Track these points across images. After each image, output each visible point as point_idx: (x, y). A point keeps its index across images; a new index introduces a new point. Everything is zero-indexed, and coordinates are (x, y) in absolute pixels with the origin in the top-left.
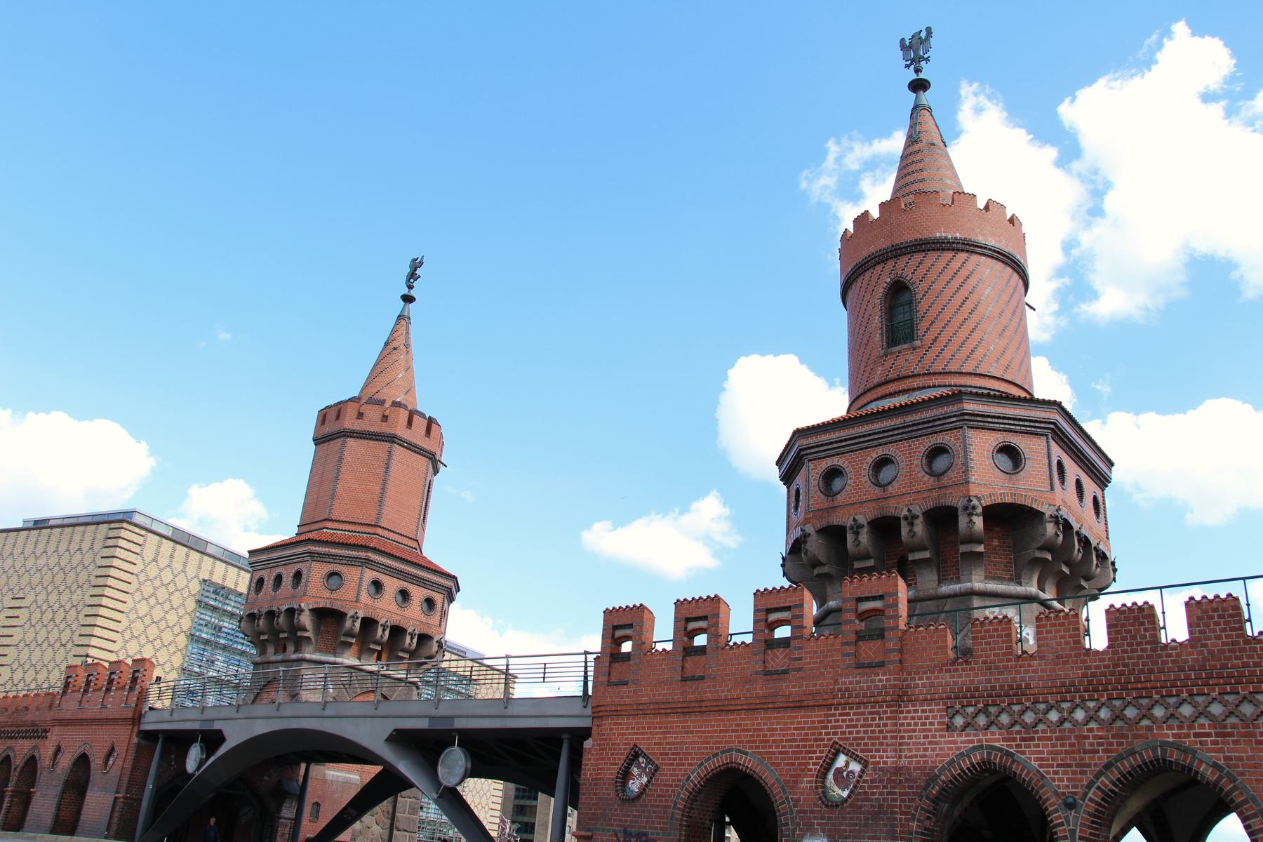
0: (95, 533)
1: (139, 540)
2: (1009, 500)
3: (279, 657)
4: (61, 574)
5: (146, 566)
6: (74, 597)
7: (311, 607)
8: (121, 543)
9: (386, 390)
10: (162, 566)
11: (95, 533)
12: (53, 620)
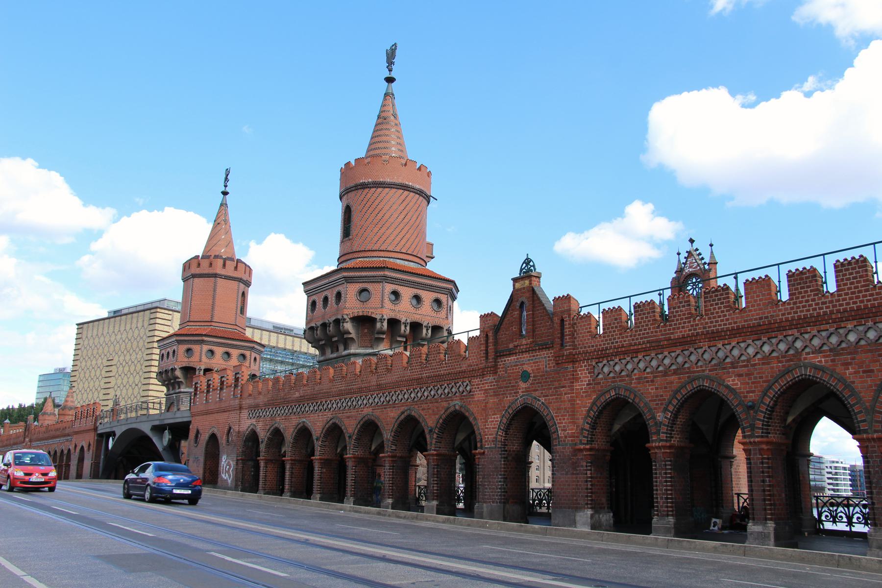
1: (169, 317)
2: (361, 314)
4: (130, 344)
6: (138, 356)
8: (158, 321)
12: (129, 371)
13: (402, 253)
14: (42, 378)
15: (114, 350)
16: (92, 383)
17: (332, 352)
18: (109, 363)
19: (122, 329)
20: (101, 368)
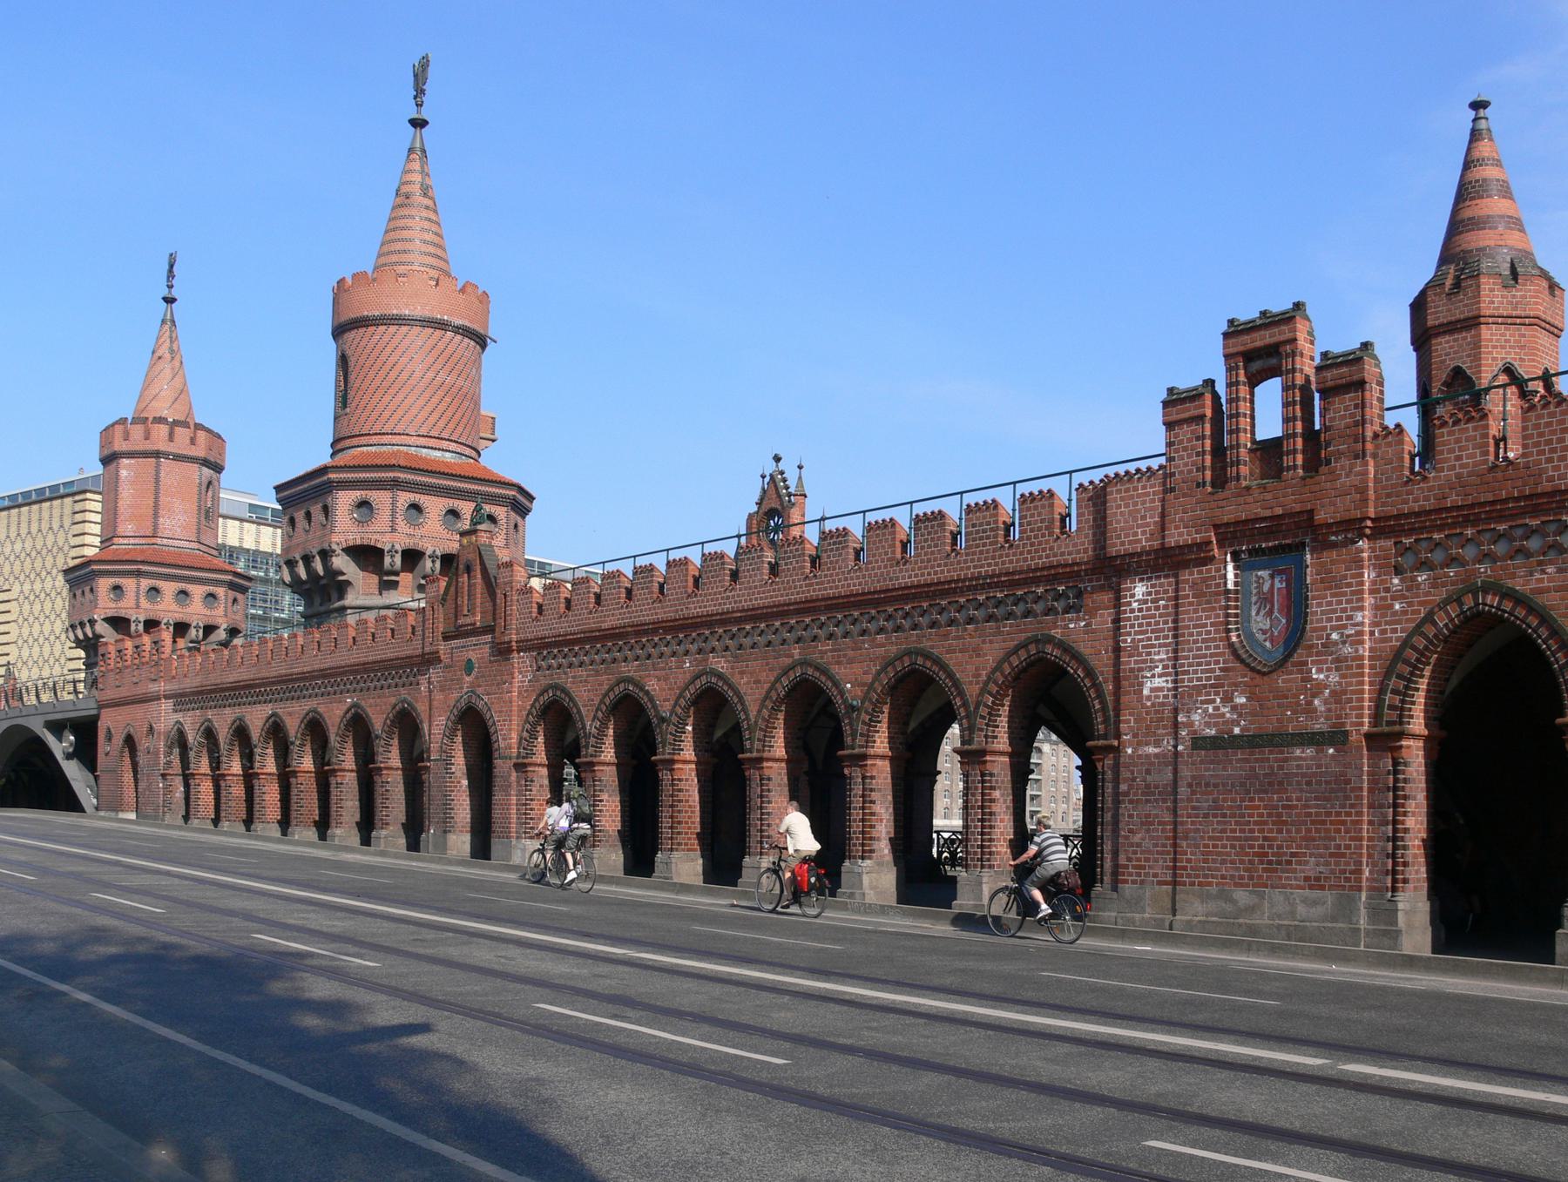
2: (359, 542)
9: (154, 403)
12: (42, 610)
13: (431, 437)
15: (12, 572)
17: (321, 605)
19: (24, 531)
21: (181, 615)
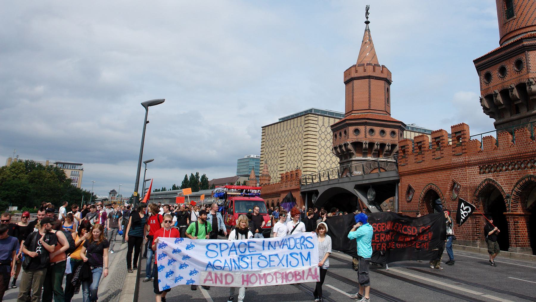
0: (301, 120)
1: (316, 119)
3: (346, 161)
4: (294, 136)
5: (320, 128)
7: (351, 142)
10: (326, 127)
11: (301, 120)
12: (294, 152)
14: (239, 162)
16: (273, 161)
18: (282, 149)
19: (288, 128)
20: (278, 152)
21: (382, 141)
